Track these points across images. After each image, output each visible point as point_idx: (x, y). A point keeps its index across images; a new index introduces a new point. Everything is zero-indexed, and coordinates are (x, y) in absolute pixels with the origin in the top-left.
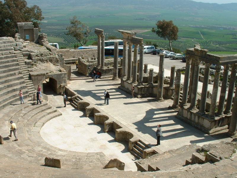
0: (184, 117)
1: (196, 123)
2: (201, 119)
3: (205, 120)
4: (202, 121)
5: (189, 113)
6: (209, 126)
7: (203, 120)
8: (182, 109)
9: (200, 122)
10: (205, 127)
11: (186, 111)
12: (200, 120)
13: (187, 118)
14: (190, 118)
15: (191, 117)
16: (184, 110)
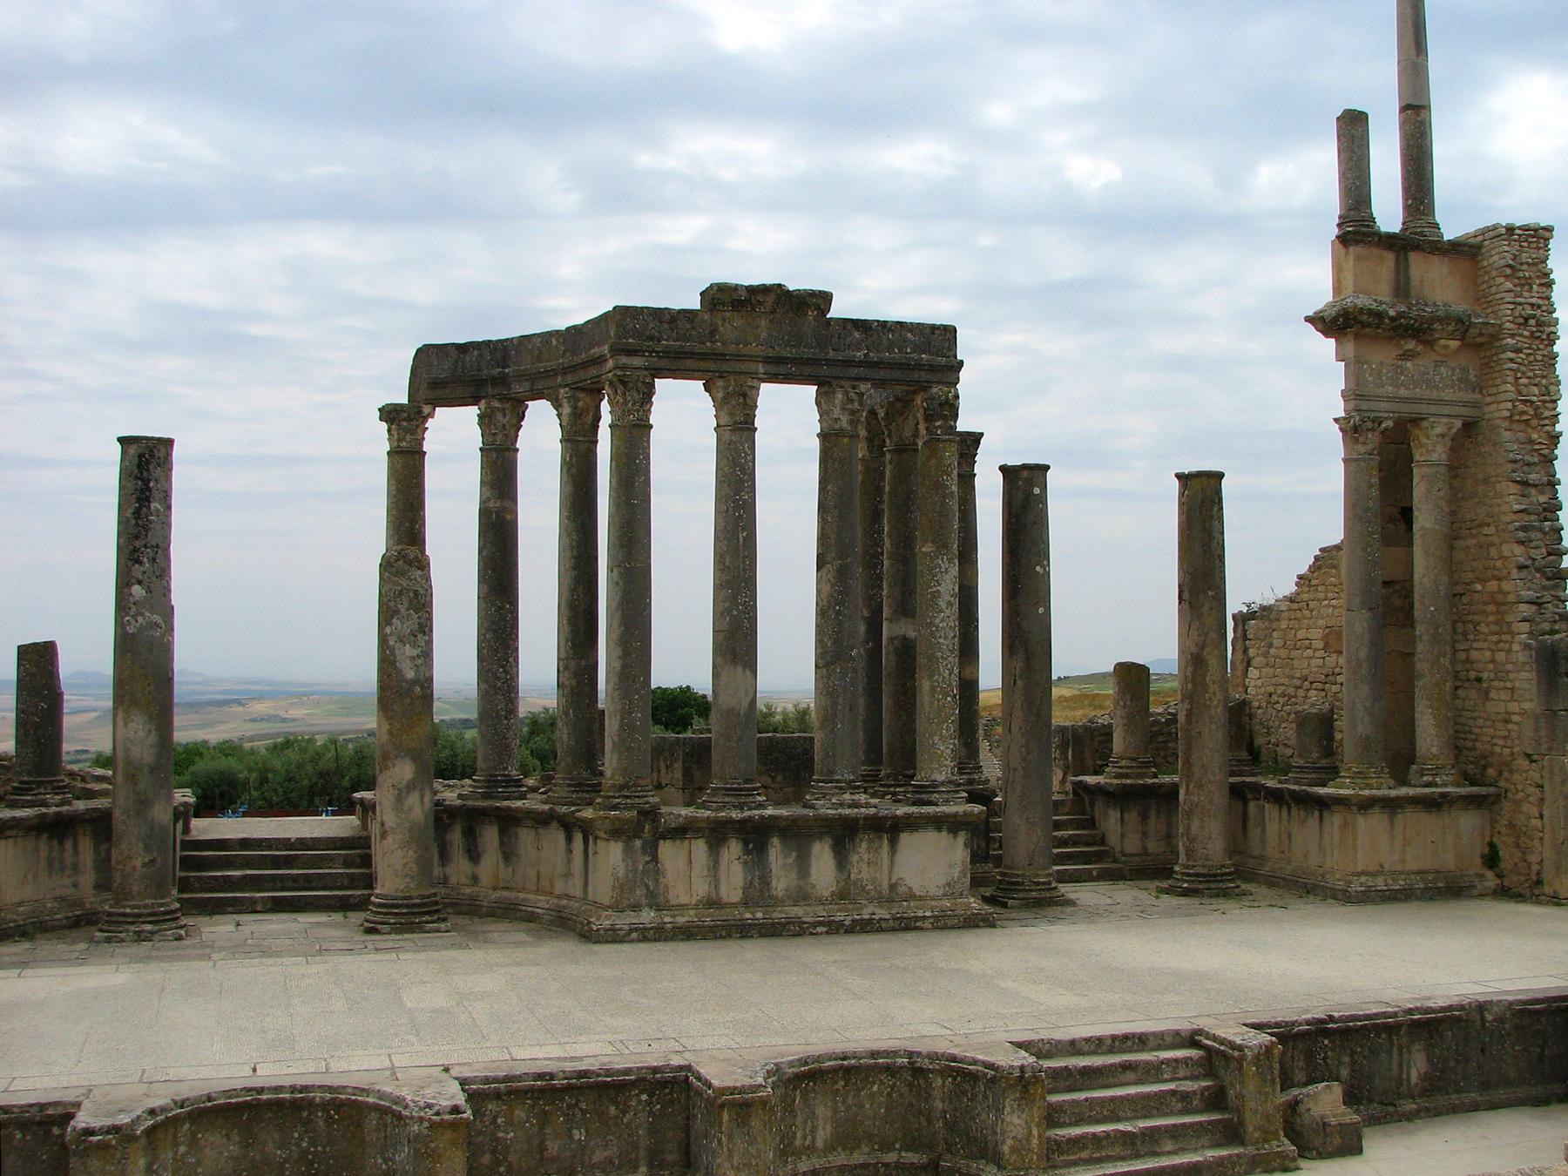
0: (683, 907)
1: (821, 901)
2: (864, 845)
3: (905, 837)
4: (886, 862)
5: (733, 851)
6: (956, 873)
7: (893, 843)
8: (638, 843)
9: (865, 875)
10: (911, 896)
11: (700, 847)
12: (855, 858)
13: (713, 903)
14: (746, 888)
15: (765, 881)
16: (666, 849)
